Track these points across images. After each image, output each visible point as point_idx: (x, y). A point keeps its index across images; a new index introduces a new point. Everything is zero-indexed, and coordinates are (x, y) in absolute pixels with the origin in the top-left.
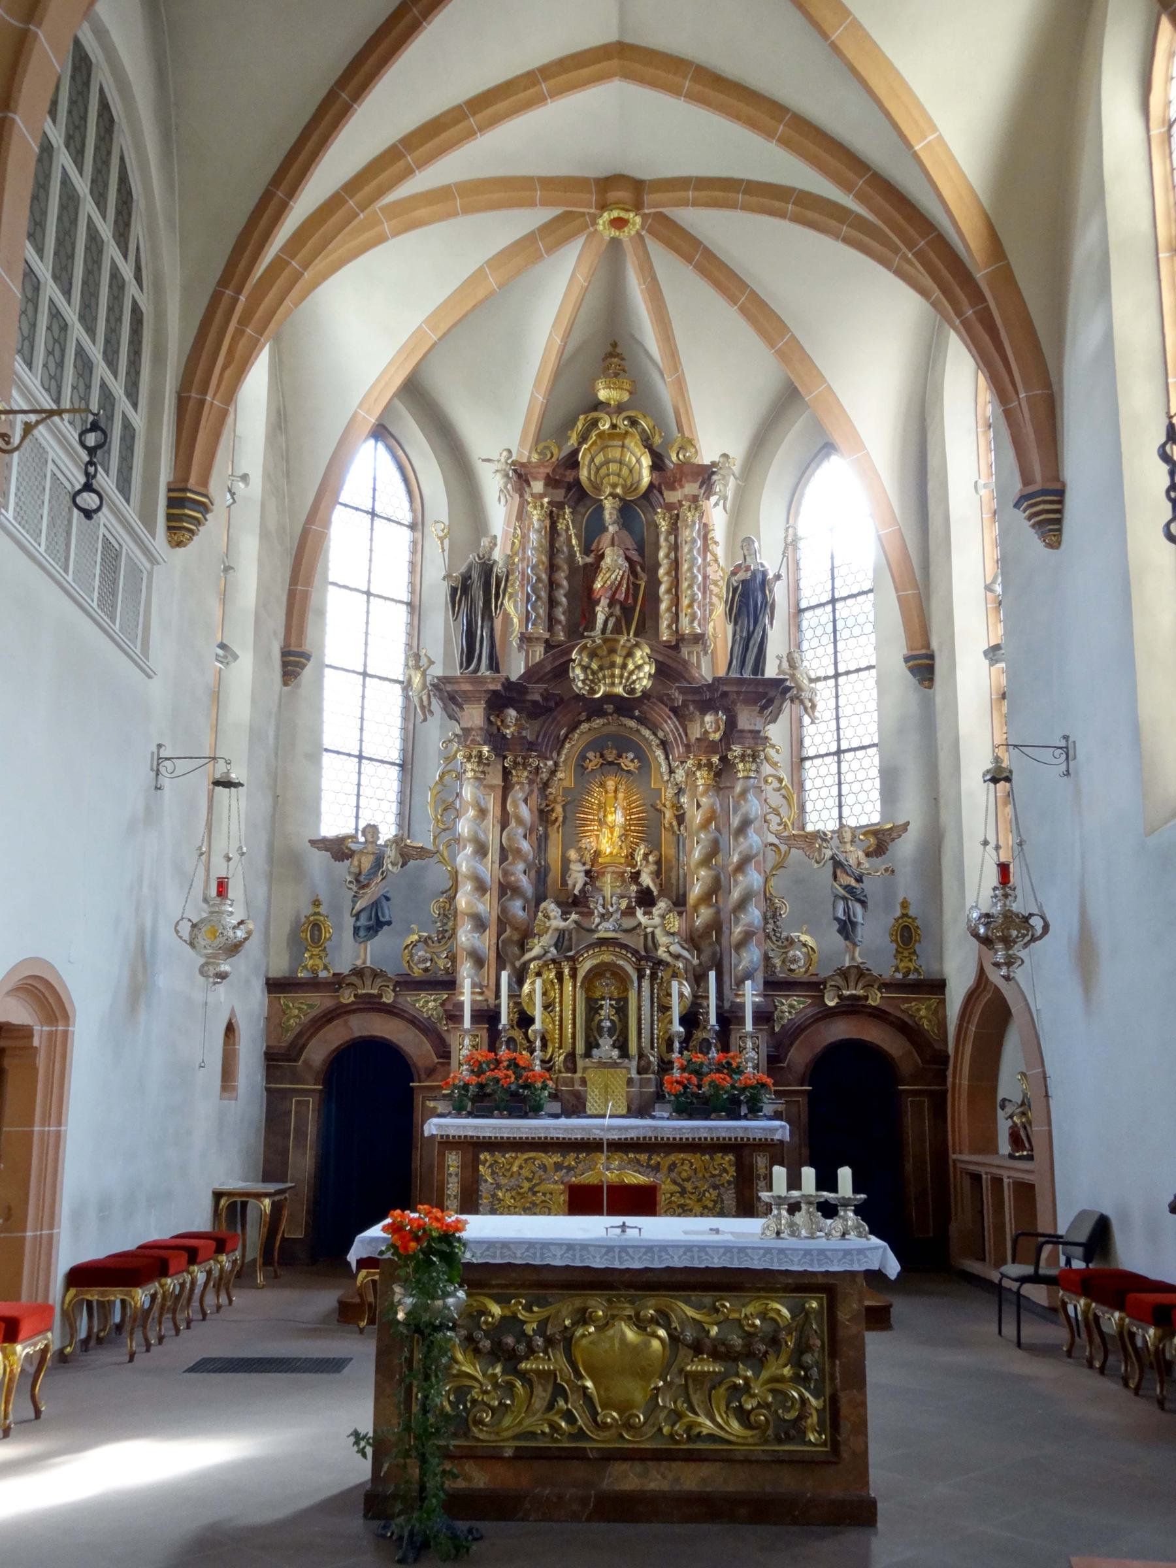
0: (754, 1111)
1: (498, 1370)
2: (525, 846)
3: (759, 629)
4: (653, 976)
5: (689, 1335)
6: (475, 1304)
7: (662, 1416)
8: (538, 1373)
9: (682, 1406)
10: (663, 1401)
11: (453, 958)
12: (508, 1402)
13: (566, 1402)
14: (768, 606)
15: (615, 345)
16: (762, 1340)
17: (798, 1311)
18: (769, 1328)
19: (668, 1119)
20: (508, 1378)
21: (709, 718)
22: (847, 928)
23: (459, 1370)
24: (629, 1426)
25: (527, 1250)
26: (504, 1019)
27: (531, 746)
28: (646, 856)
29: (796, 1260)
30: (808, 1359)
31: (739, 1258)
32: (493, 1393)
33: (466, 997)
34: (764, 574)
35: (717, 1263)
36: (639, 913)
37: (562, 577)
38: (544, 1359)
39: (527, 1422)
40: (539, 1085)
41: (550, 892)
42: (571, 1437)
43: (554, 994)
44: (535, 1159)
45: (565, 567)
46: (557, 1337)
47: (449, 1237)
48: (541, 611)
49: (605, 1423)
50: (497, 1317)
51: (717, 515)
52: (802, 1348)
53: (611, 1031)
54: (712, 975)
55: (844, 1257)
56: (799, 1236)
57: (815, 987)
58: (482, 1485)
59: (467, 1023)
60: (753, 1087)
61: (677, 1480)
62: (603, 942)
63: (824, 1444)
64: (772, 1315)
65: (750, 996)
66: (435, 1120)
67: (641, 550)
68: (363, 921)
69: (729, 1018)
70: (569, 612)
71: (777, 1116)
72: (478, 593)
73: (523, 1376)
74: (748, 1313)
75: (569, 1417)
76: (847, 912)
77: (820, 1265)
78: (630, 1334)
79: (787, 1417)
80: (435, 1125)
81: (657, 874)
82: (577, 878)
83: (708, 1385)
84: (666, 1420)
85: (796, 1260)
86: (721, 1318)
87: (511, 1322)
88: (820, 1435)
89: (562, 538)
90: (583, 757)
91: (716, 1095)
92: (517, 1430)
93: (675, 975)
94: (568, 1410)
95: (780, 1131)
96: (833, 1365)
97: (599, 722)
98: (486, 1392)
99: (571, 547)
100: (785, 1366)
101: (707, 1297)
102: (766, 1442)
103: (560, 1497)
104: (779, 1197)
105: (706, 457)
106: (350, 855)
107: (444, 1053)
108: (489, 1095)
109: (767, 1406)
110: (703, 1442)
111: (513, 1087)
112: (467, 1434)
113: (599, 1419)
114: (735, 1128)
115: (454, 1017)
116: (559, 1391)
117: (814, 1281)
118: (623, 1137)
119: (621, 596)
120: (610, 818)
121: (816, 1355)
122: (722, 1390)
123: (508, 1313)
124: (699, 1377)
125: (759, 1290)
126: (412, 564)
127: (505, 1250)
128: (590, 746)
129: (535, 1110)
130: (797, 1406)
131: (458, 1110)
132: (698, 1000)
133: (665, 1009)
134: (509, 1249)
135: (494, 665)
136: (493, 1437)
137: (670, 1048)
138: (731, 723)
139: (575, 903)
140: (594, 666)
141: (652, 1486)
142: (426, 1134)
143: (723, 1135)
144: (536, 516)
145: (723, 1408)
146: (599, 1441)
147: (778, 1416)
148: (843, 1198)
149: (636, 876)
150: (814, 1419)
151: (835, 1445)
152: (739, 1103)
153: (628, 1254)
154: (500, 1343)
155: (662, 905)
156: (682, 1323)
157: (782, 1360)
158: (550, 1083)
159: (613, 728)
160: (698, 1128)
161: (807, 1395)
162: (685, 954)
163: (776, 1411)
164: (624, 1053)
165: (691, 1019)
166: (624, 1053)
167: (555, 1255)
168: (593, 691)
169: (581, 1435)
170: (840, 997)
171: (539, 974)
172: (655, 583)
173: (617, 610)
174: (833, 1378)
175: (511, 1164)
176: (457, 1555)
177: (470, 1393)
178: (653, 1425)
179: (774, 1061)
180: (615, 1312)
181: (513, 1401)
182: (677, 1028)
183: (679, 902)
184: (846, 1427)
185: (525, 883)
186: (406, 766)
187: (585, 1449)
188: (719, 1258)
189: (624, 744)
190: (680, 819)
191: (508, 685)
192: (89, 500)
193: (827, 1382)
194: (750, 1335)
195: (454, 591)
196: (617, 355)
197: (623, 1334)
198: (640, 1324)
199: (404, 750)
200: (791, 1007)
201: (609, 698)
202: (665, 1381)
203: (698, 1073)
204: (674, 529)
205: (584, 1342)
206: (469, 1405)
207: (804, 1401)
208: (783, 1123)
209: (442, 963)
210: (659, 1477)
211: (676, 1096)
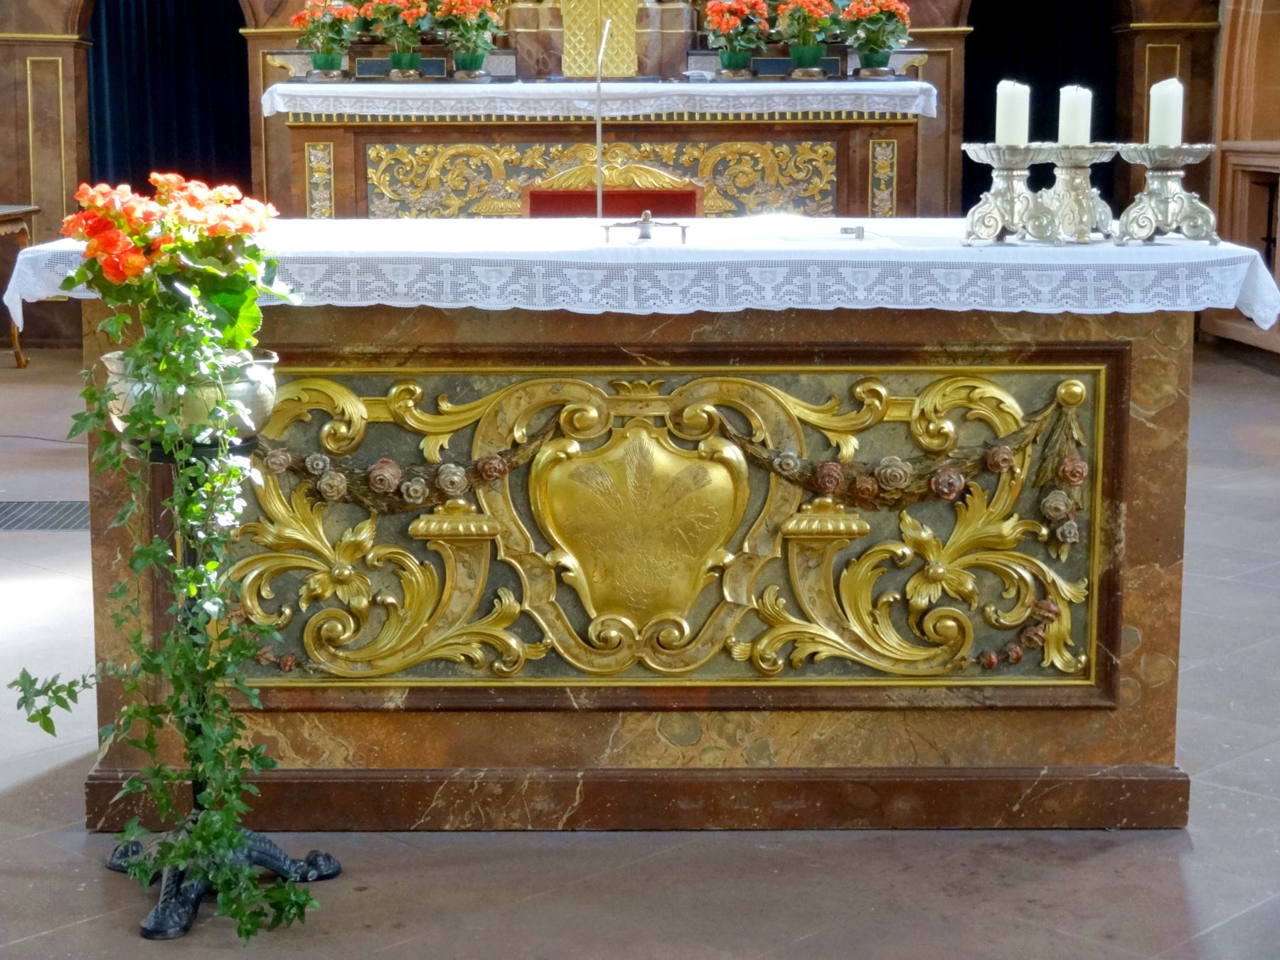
0: (873, 61)
1: (366, 533)
5: (794, 456)
6: (305, 397)
7: (731, 622)
8: (456, 540)
9: (774, 601)
10: (734, 591)
12: (391, 600)
13: (520, 600)
16: (957, 463)
18: (972, 439)
19: (713, 81)
20: (384, 551)
23: (279, 537)
24: (659, 645)
25: (422, 276)
29: (1045, 290)
30: (1058, 501)
31: (914, 288)
32: (357, 583)
35: (863, 299)
38: (467, 512)
39: (433, 639)
40: (472, 19)
42: (535, 667)
44: (469, 155)
46: (495, 463)
49: (606, 640)
50: (359, 425)
55: (1157, 281)
56: (1052, 240)
58: (339, 764)
60: (872, 21)
61: (762, 748)
63: (1085, 672)
64: (982, 410)
66: (280, 88)
73: (422, 546)
74: (929, 408)
75: (527, 627)
77: (1102, 301)
78: (663, 458)
79: (1008, 619)
80: (283, 95)
83: (834, 559)
84: (739, 629)
85: (1045, 290)
86: (866, 418)
88: (1075, 655)
91: (804, 36)
92: (413, 656)
94: (524, 613)
95: (920, 100)
96: (1115, 513)
98: (340, 581)
100: (1007, 517)
101: (837, 378)
102: (958, 670)
103: (509, 787)
104: (1013, 150)
108: (382, 41)
109: (965, 599)
110: (821, 673)
111: (425, 26)
112: (302, 663)
113: (592, 631)
114: (837, 95)
116: (504, 575)
117: (1081, 336)
118: (631, 113)
121: (1076, 493)
122: (865, 568)
123: (383, 415)
124: (813, 544)
125: (954, 357)
127: (370, 278)
129: (468, 67)
130: (1029, 598)
131: (326, 67)
134: (380, 275)
136: (360, 670)
141: (709, 760)
142: (267, 111)
143: (815, 107)
145: (866, 606)
147: (987, 621)
148: (1164, 150)
150: (1062, 625)
151: (1108, 677)
152: (844, 52)
153: (656, 283)
154: (366, 480)
156: (777, 432)
157: (1001, 505)
158: (495, 18)
160: (770, 96)
161: (1051, 575)
163: (982, 610)
167: (485, 288)
169: (554, 660)
174: (1110, 541)
175: (426, 166)
176: (277, 920)
177: (304, 582)
178: (712, 641)
180: (626, 410)
181: (402, 597)
184: (1131, 636)
187: (562, 689)
188: (869, 289)
193: (1098, 548)
194: (929, 453)
197: (644, 454)
202: (738, 550)
205: (557, 474)
206: (304, 606)
207: (1043, 588)
208: (926, 85)
210: (722, 742)
211: (730, 39)
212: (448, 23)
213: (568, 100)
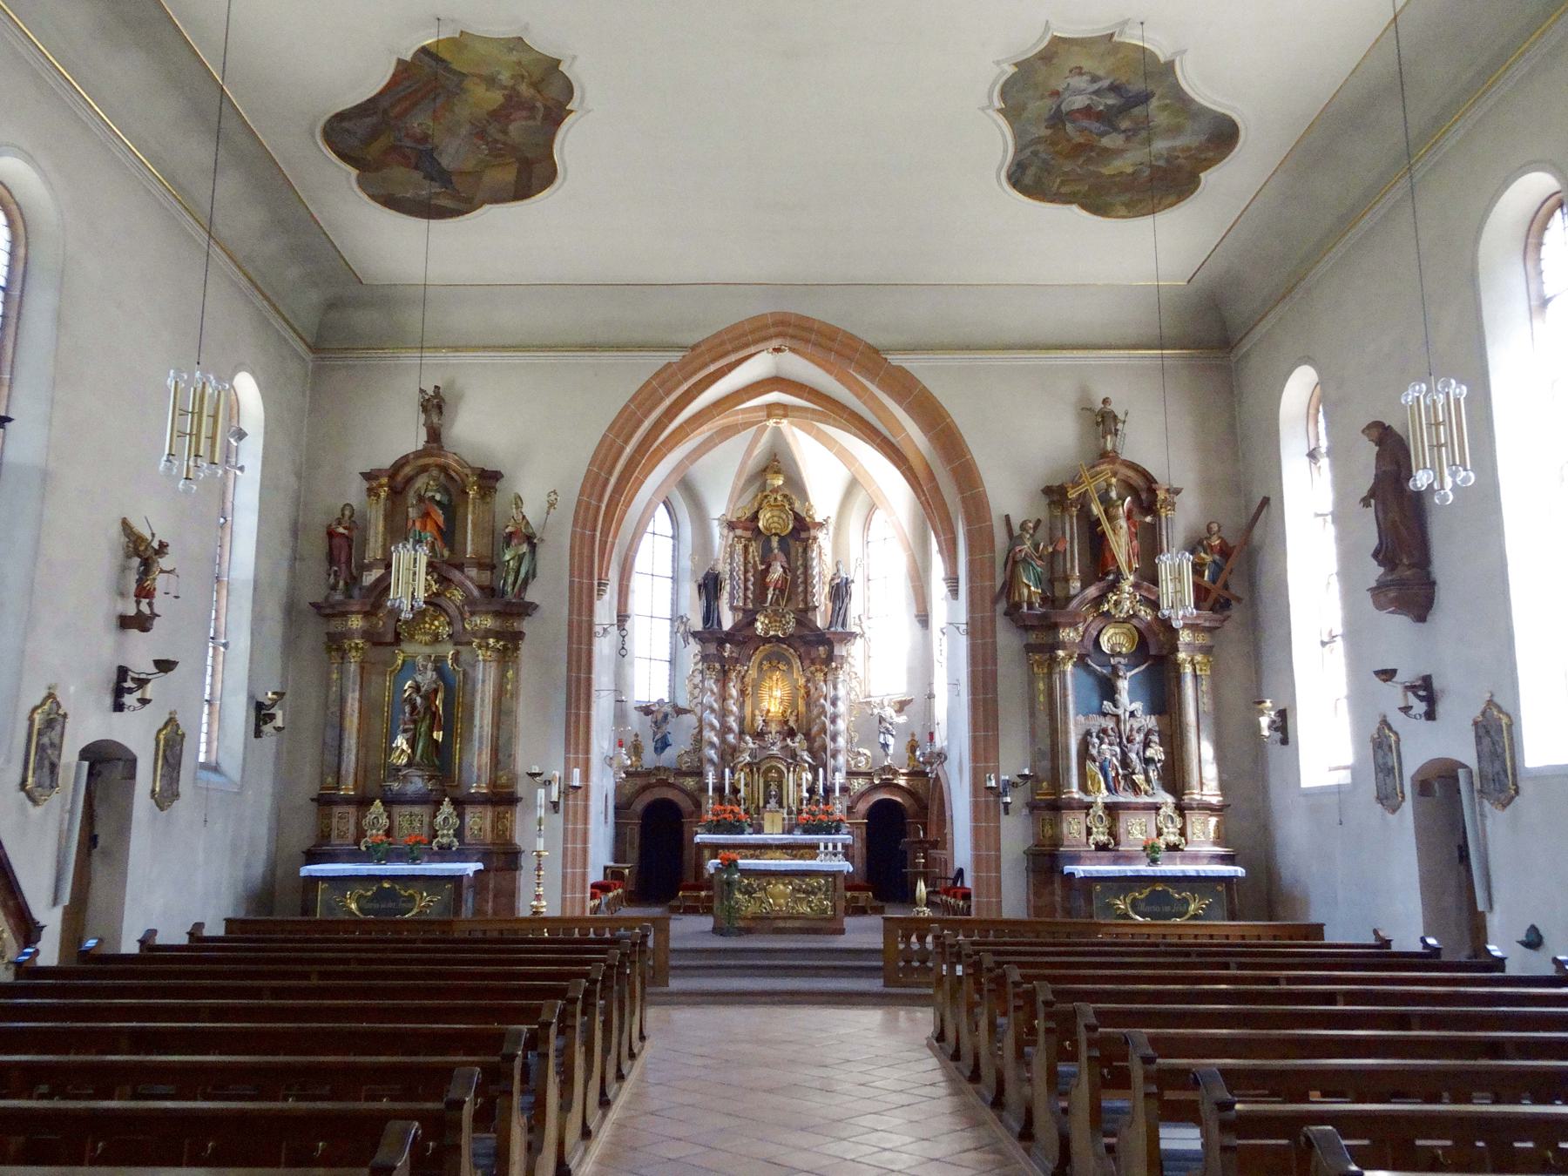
2: (735, 709)
3: (845, 604)
4: (794, 771)
11: (700, 760)
14: (848, 593)
15: (775, 455)
17: (826, 881)
21: (821, 648)
22: (885, 746)
26: (727, 791)
27: (737, 660)
28: (791, 713)
33: (711, 779)
34: (847, 579)
36: (788, 740)
37: (750, 575)
41: (746, 730)
43: (749, 779)
45: (752, 570)
47: (735, 861)
48: (741, 594)
51: (824, 539)
52: (827, 890)
53: (775, 796)
54: (821, 770)
57: (868, 775)
59: (711, 793)
62: (772, 757)
65: (839, 779)
67: (789, 563)
68: (659, 745)
69: (828, 790)
70: (753, 593)
71: (848, 833)
72: (711, 586)
73: (754, 898)
76: (885, 739)
78: (781, 887)
81: (797, 721)
82: (759, 722)
87: (750, 884)
89: (750, 556)
90: (761, 664)
93: (804, 770)
97: (767, 646)
99: (755, 562)
105: (818, 519)
106: (652, 712)
107: (698, 805)
115: (704, 789)
119: (779, 585)
120: (775, 693)
126: (673, 557)
128: (763, 659)
131: (709, 832)
132: (816, 778)
133: (799, 785)
135: (719, 623)
137: (802, 804)
138: (831, 651)
139: (759, 735)
140: (767, 622)
144: (739, 548)
146: (774, 915)
149: (786, 722)
155: (799, 737)
159: (776, 649)
162: (810, 760)
164: (781, 806)
165: (811, 790)
166: (781, 806)
168: (766, 633)
170: (881, 779)
171: (742, 770)
172: (795, 577)
173: (777, 592)
179: (850, 809)
182: (806, 795)
183: (807, 736)
185: (735, 726)
186: (673, 662)
189: (781, 658)
190: (808, 693)
191: (727, 633)
192: (623, 652)
195: (700, 586)
196: (777, 461)
198: (785, 885)
199: (671, 654)
200: (859, 784)
201: (772, 637)
203: (813, 815)
204: (805, 551)
209: (697, 764)
212: (738, 821)
213: (766, 839)
